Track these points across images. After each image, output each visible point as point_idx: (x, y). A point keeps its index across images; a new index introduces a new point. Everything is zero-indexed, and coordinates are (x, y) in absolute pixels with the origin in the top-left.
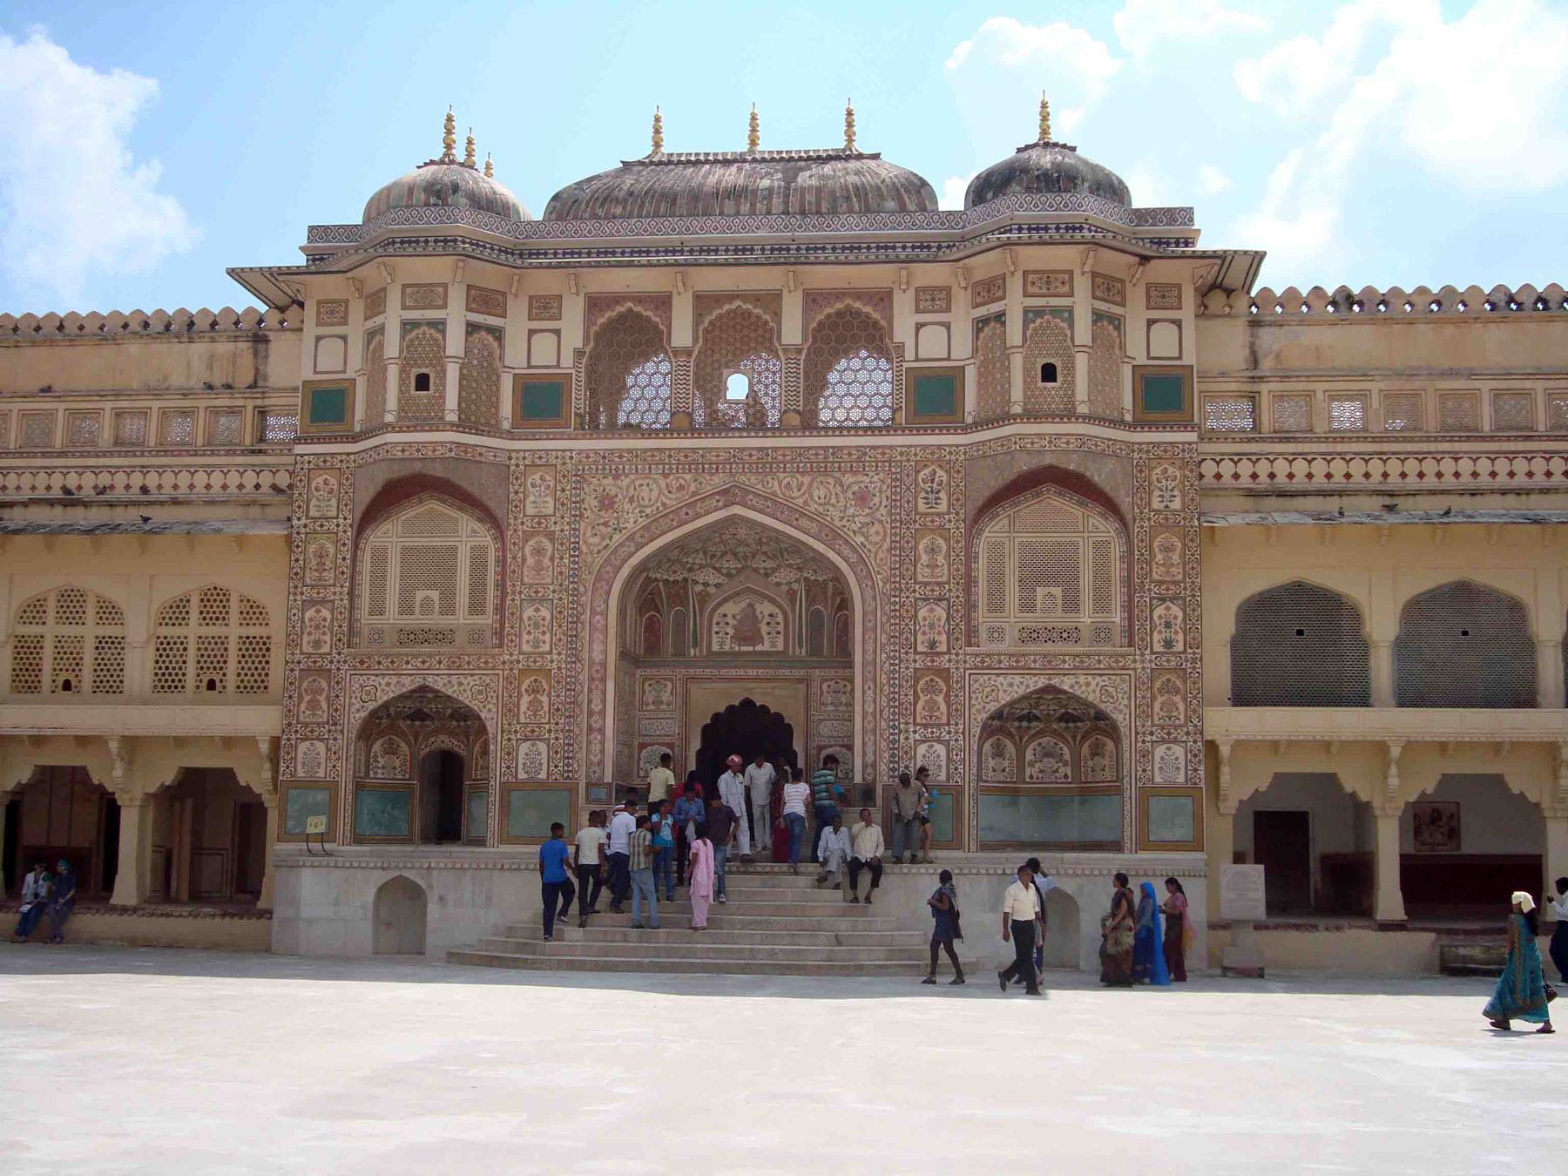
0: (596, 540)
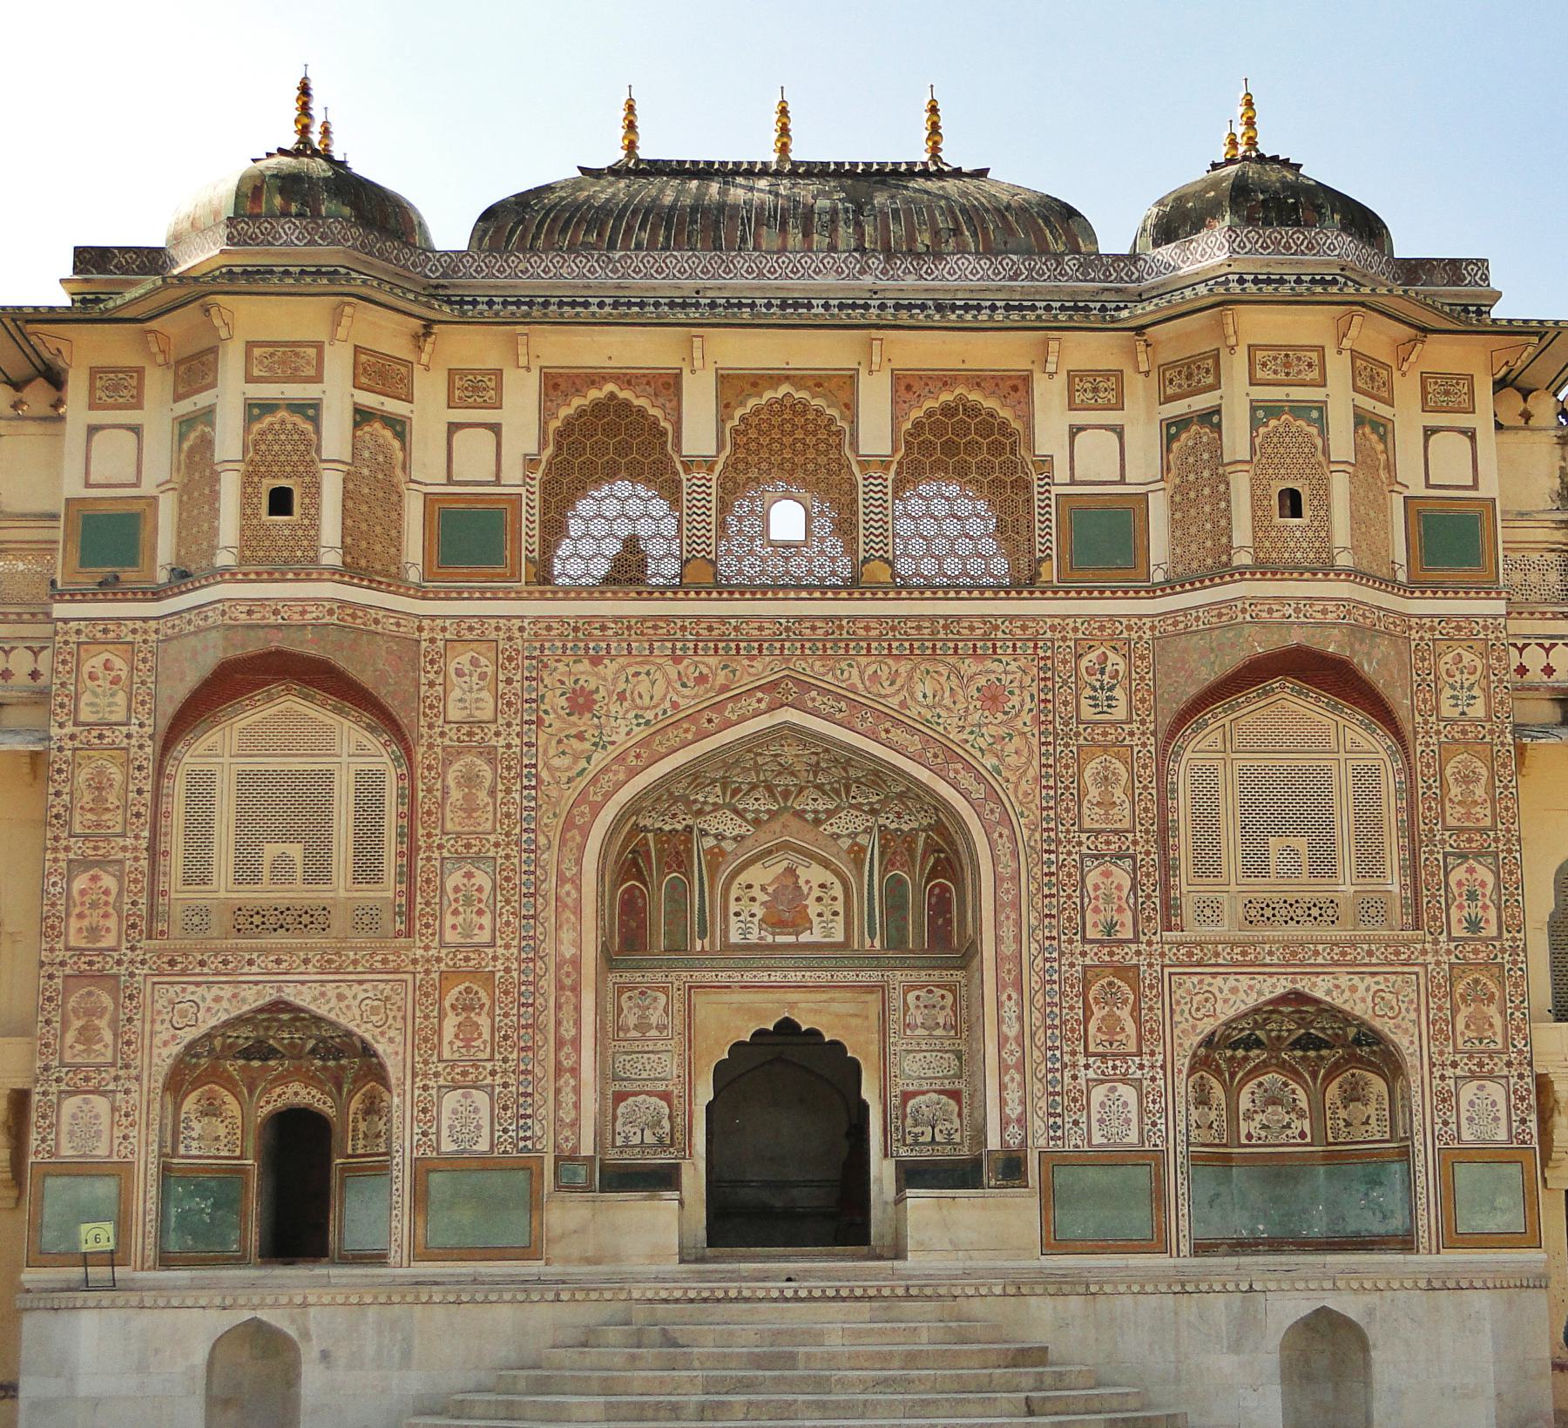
0: (565, 761)
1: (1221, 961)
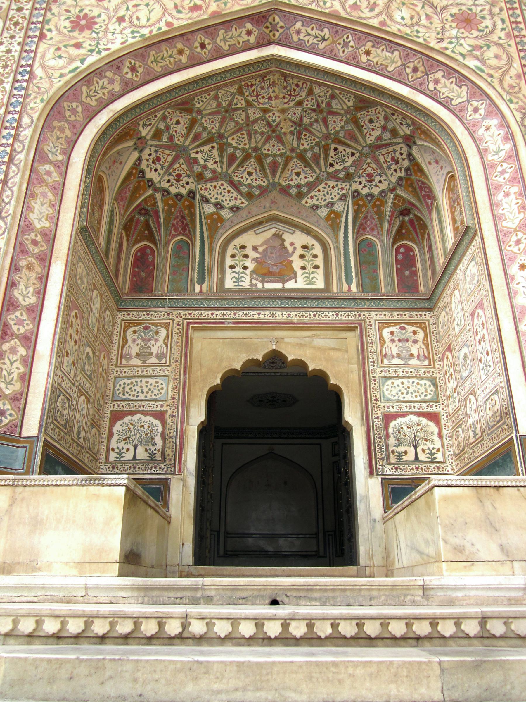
0: (60, 63)
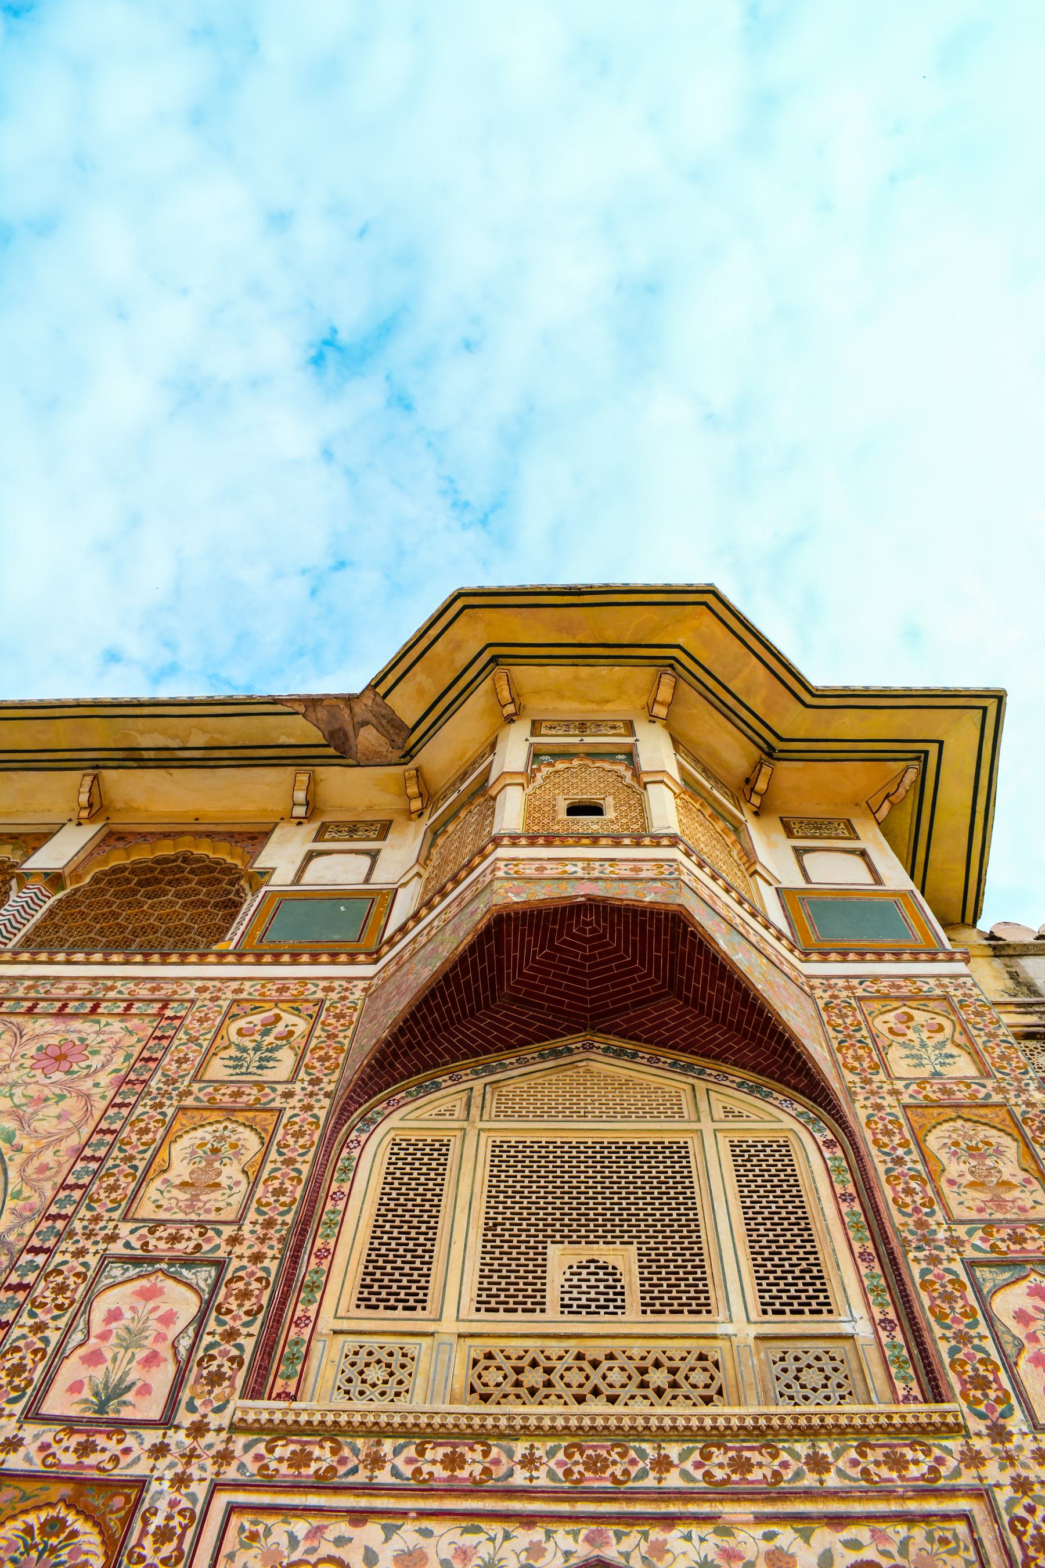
1: (384, 1477)
